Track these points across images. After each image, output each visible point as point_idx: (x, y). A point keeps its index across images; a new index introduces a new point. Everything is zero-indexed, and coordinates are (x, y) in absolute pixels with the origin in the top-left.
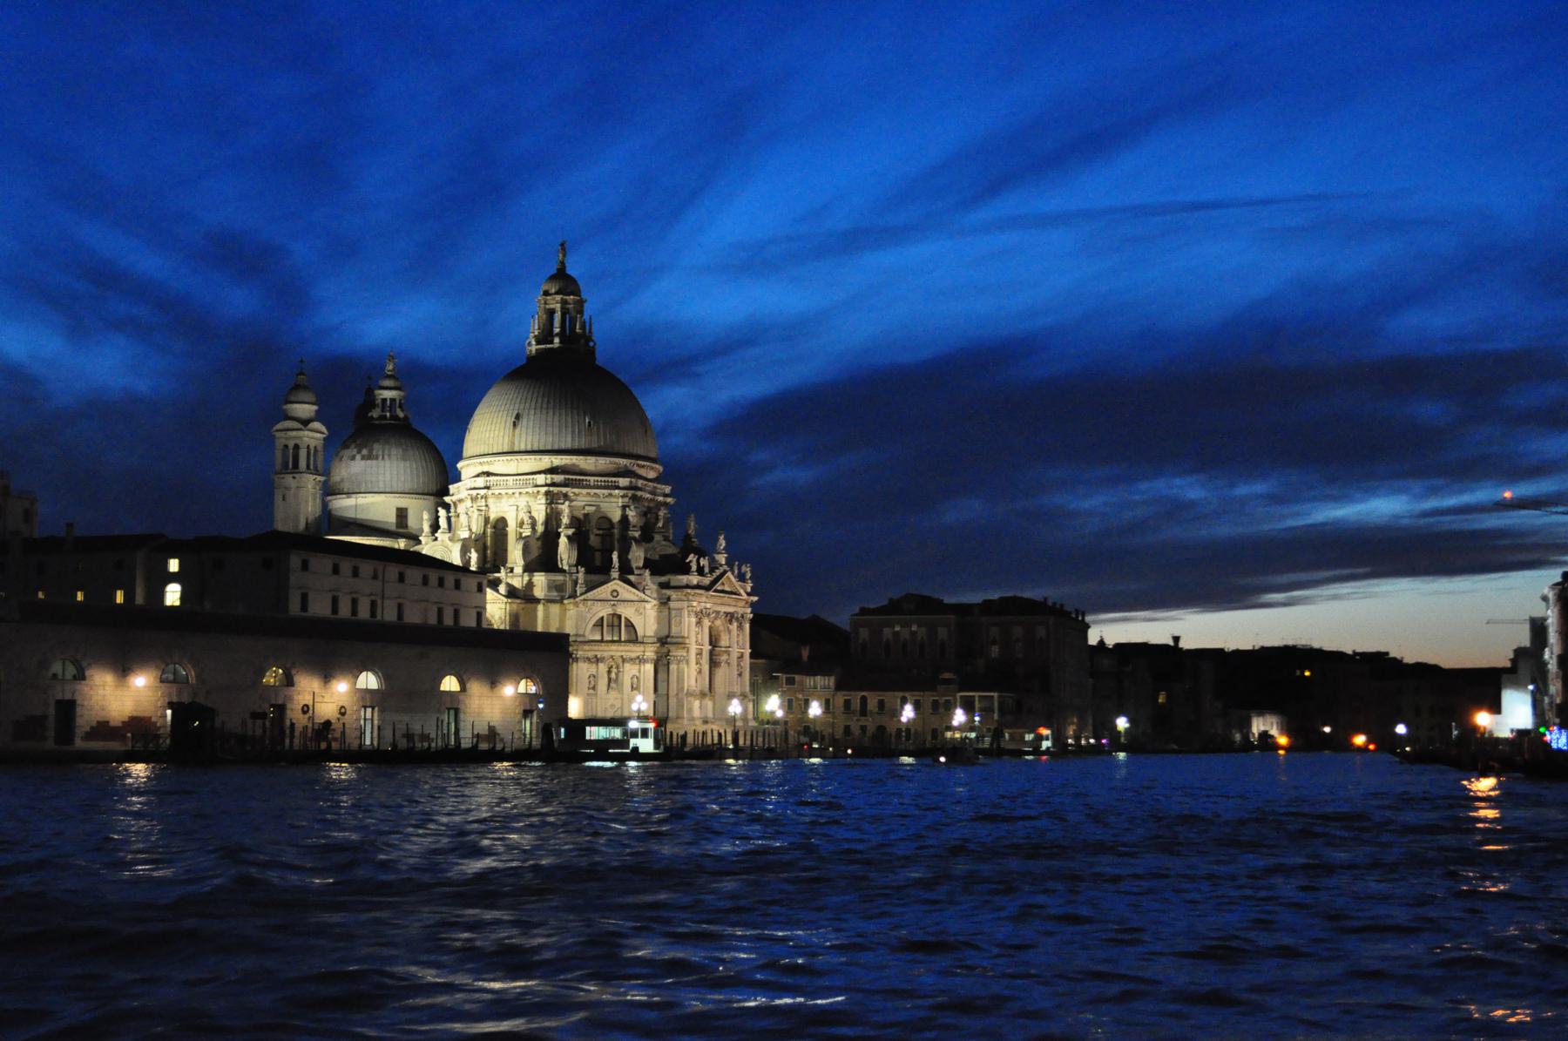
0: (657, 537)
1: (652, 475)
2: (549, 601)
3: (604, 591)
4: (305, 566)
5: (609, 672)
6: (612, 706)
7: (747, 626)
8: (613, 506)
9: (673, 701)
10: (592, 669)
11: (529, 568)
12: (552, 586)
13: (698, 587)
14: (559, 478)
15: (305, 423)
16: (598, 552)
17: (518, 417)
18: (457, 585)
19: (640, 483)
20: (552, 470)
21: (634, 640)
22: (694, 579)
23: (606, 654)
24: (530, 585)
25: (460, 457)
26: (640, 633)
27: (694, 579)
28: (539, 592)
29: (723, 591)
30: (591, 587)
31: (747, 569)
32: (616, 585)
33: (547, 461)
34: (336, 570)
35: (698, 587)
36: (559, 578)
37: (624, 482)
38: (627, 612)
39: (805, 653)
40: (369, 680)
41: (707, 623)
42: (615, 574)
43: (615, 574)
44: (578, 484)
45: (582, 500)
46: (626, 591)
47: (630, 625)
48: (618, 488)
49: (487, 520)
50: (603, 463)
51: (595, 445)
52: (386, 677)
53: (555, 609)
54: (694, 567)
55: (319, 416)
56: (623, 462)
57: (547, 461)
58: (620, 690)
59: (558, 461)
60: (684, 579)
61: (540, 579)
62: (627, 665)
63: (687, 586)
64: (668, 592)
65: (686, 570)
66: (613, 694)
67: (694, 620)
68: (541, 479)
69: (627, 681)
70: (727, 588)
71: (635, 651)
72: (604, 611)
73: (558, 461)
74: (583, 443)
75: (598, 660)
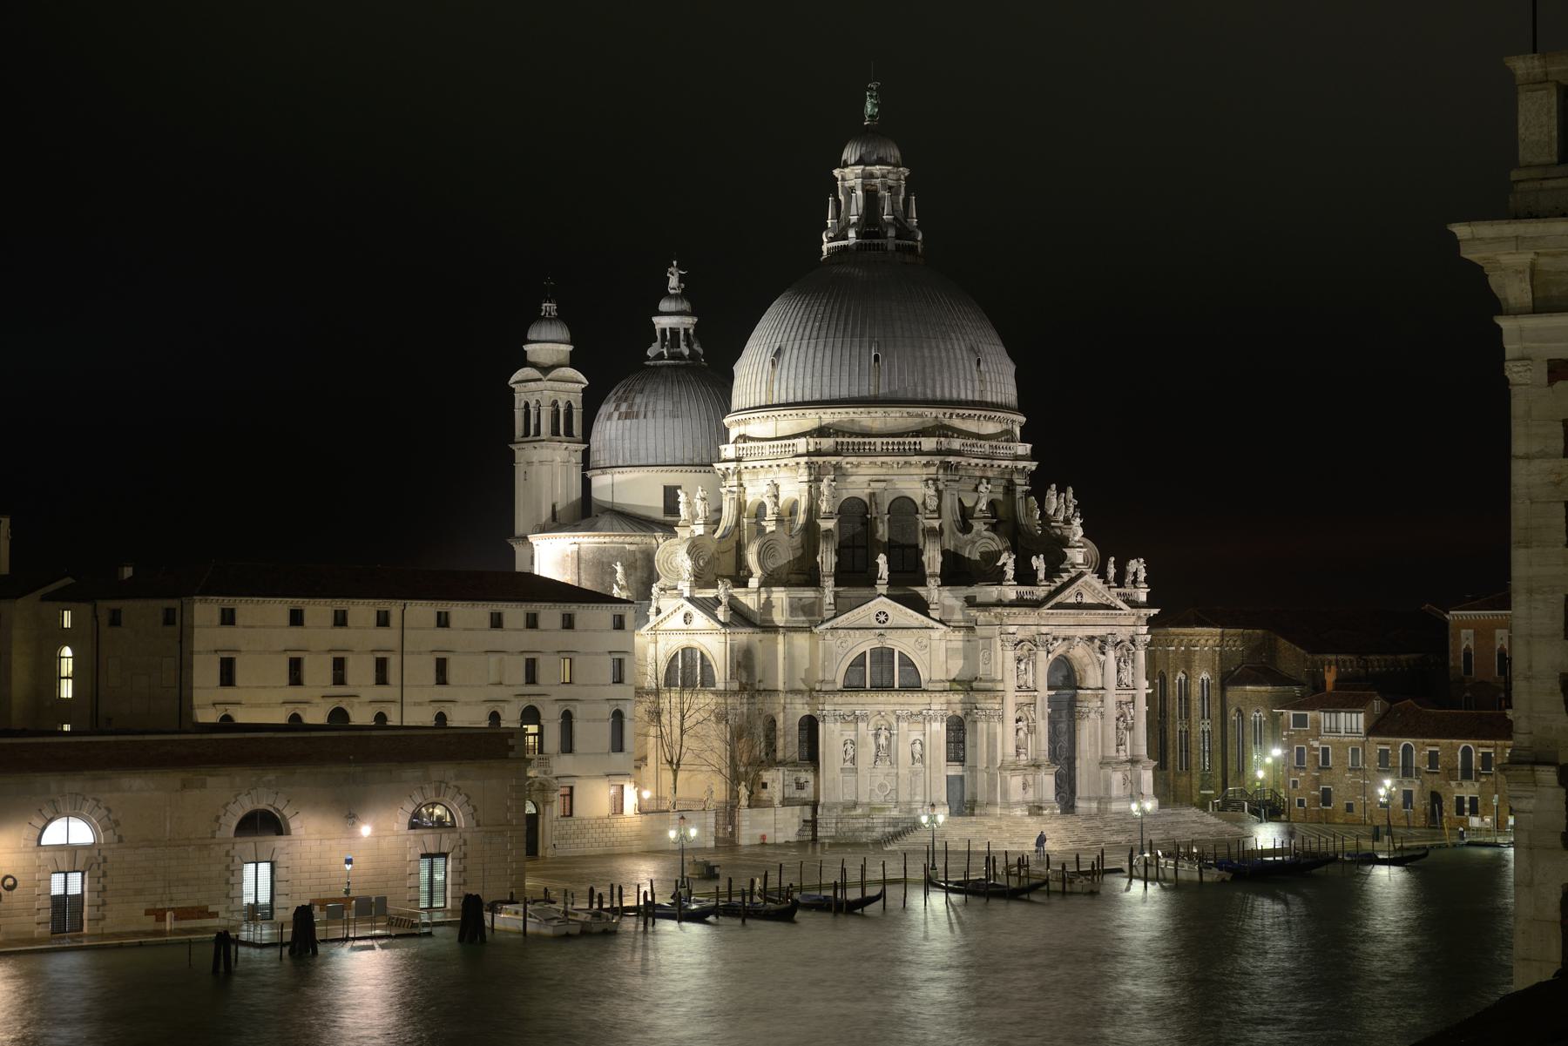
0: (979, 526)
1: (990, 428)
2: (790, 629)
3: (865, 613)
4: (228, 618)
5: (877, 736)
6: (881, 786)
7: (1141, 654)
8: (913, 483)
9: (982, 778)
11: (769, 581)
12: (795, 607)
13: (1020, 603)
14: (827, 443)
15: (546, 369)
16: (860, 551)
17: (778, 353)
18: (568, 623)
19: (956, 444)
20: (821, 432)
21: (913, 686)
22: (1010, 592)
23: (869, 709)
24: (768, 605)
25: (727, 410)
26: (924, 676)
27: (1010, 592)
28: (779, 618)
29: (1079, 606)
30: (841, 608)
31: (1137, 566)
32: (882, 604)
33: (812, 419)
34: (296, 618)
35: (1020, 603)
36: (808, 594)
37: (928, 444)
38: (900, 643)
39: (1330, 677)
40: (73, 831)
41: (1043, 661)
42: (882, 588)
43: (882, 588)
44: (858, 452)
45: (863, 478)
46: (901, 614)
47: (906, 662)
48: (920, 453)
49: (741, 507)
50: (894, 418)
51: (883, 391)
52: (108, 823)
53: (801, 641)
54: (1010, 573)
55: (575, 361)
56: (931, 414)
57: (812, 419)
58: (894, 763)
59: (829, 416)
60: (992, 592)
61: (780, 595)
62: (904, 725)
63: (1000, 603)
64: (973, 612)
65: (998, 578)
66: (883, 767)
67: (1010, 655)
68: (801, 445)
69: (904, 752)
70: (1087, 599)
72: (866, 644)
73: (829, 416)
74: (866, 390)
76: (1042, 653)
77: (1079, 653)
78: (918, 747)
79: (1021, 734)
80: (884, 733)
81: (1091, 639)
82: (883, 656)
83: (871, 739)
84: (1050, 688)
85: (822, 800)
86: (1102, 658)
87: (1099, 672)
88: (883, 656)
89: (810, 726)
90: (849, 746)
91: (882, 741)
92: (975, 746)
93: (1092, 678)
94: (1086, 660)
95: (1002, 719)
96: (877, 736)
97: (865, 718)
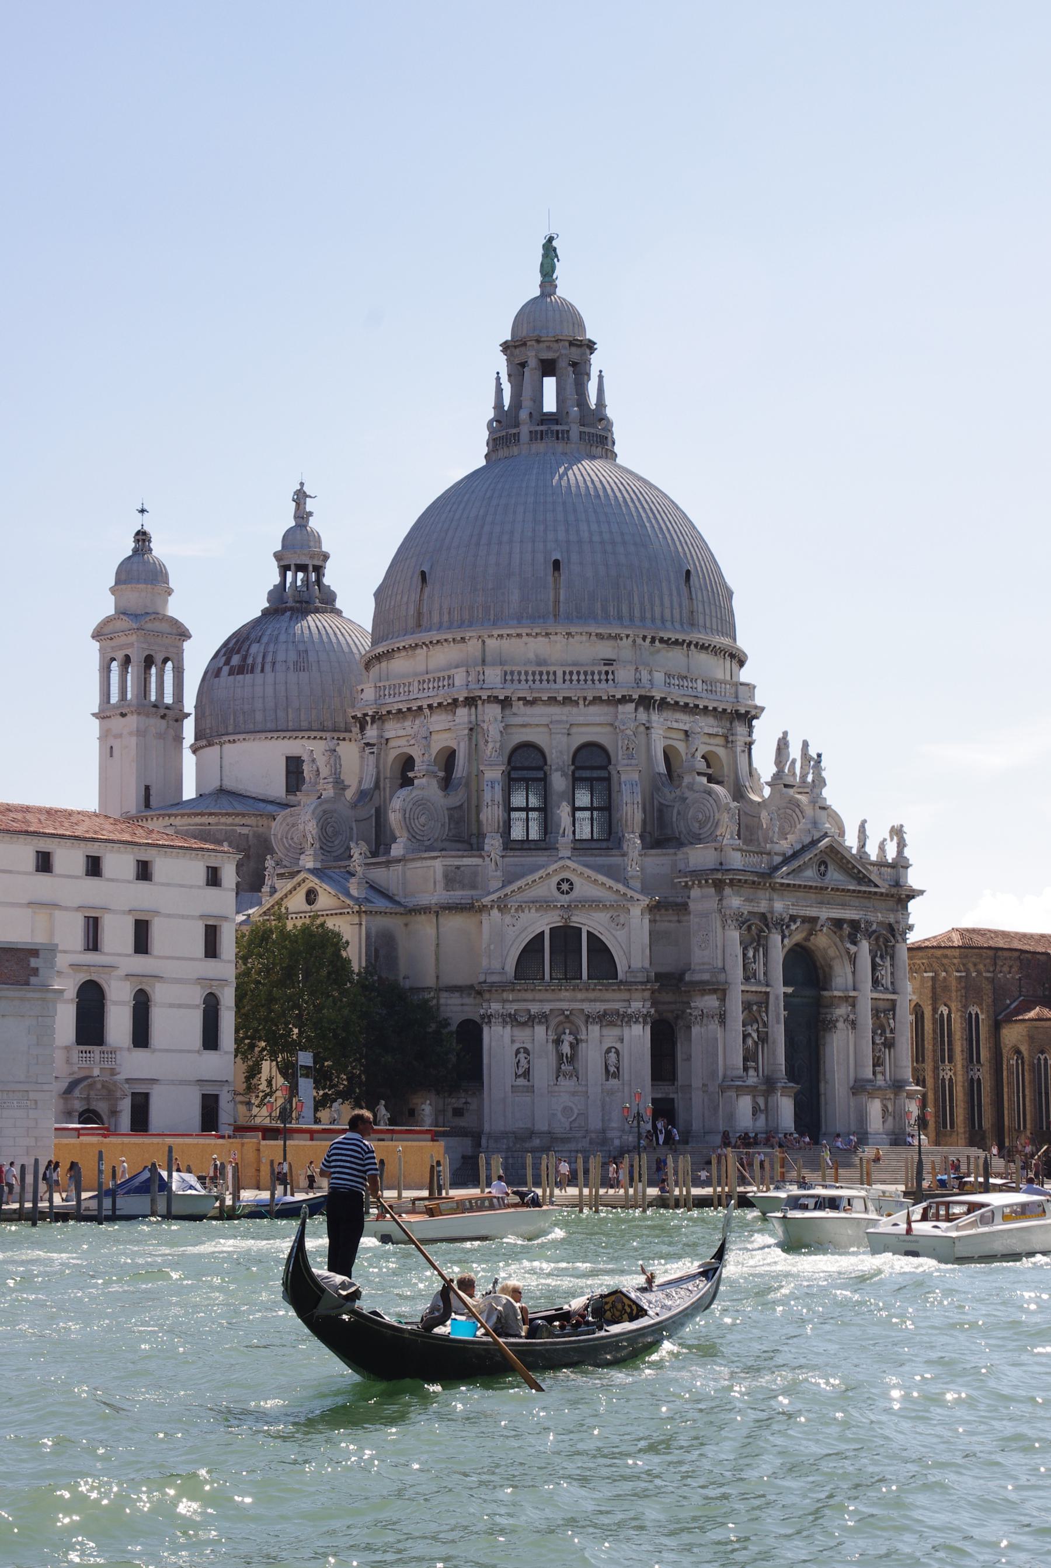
5: (558, 1042)
10: (523, 1035)
38: (590, 922)
47: (599, 949)
62: (595, 1030)
67: (735, 935)
71: (613, 1001)
72: (543, 923)
75: (532, 1020)
76: (776, 938)
77: (822, 941)
78: (613, 1055)
79: (750, 1042)
80: (568, 1038)
81: (838, 923)
82: (566, 938)
83: (551, 1047)
84: (785, 984)
85: (486, 1128)
86: (853, 949)
87: (849, 969)
88: (566, 938)
89: (471, 1034)
90: (522, 1056)
91: (566, 1049)
92: (688, 1059)
93: (841, 977)
94: (832, 952)
95: (722, 1019)
96: (558, 1042)
97: (543, 1018)
